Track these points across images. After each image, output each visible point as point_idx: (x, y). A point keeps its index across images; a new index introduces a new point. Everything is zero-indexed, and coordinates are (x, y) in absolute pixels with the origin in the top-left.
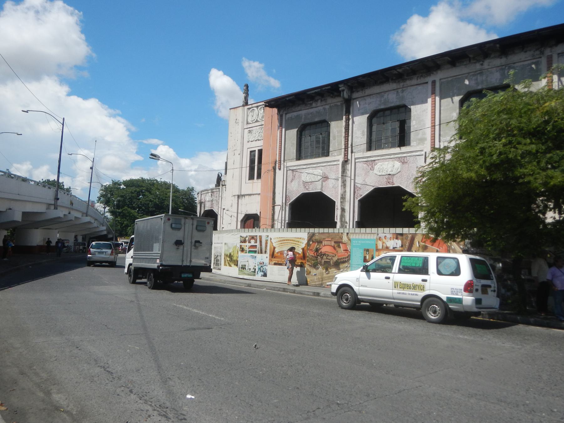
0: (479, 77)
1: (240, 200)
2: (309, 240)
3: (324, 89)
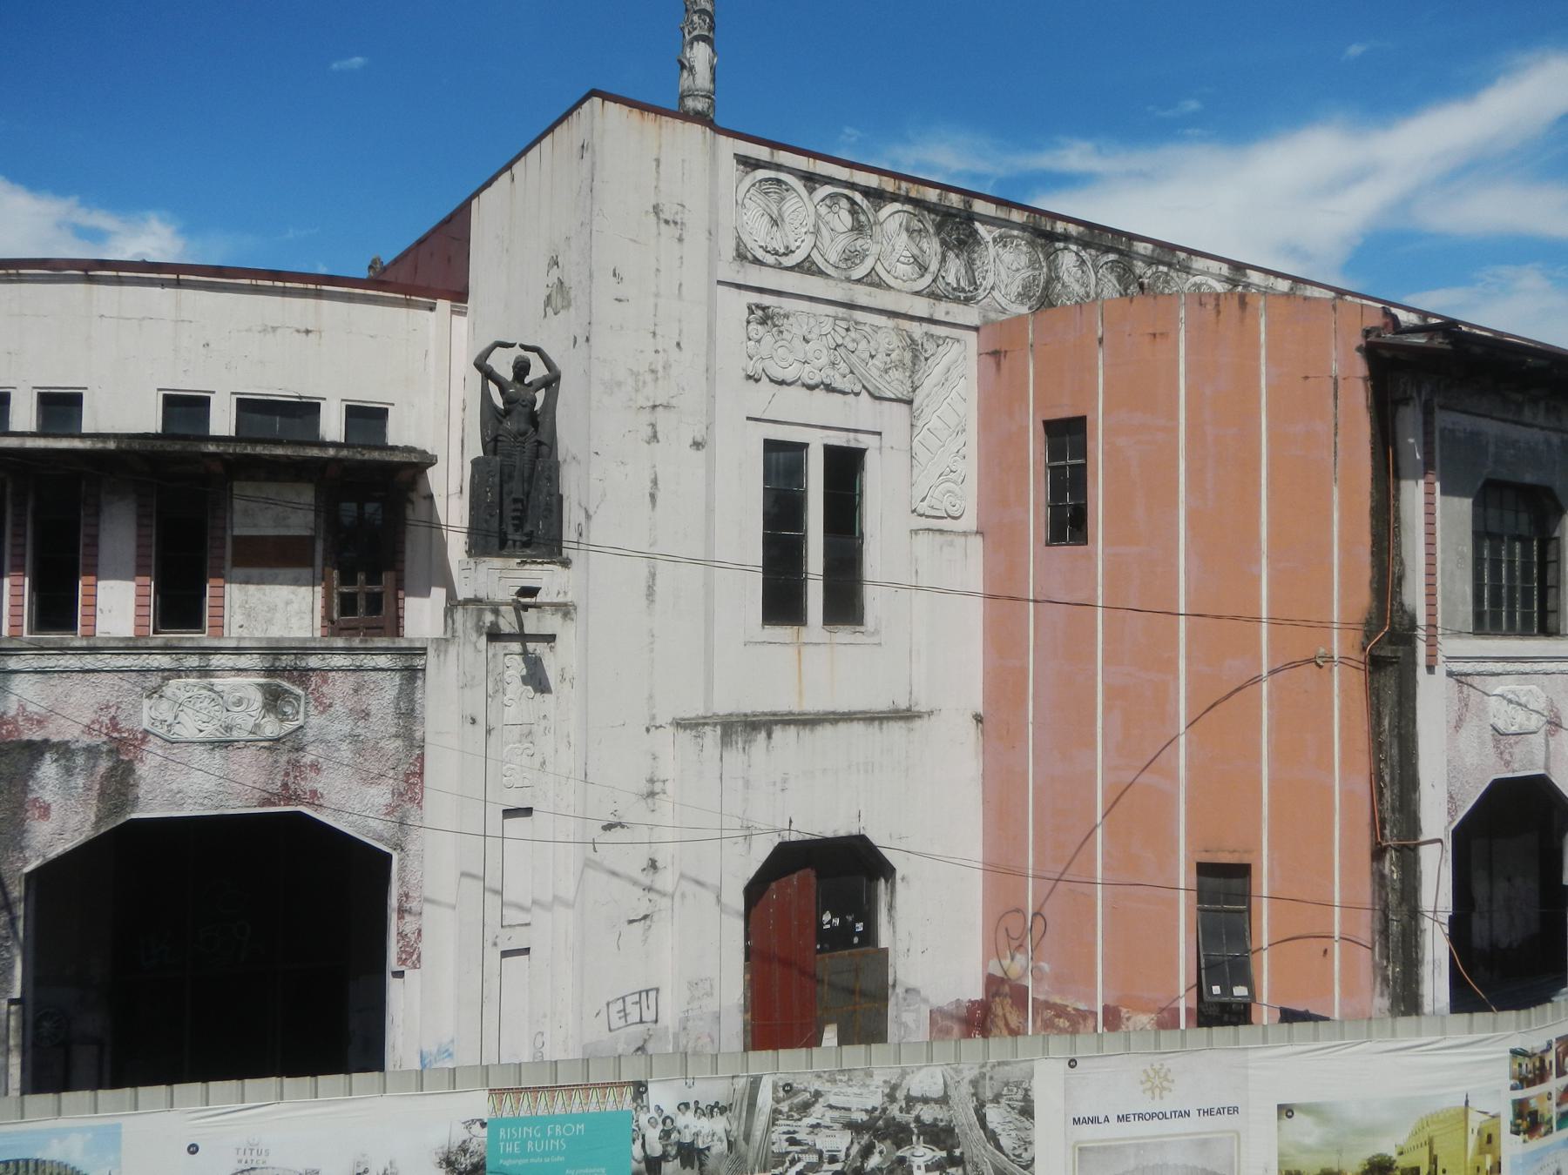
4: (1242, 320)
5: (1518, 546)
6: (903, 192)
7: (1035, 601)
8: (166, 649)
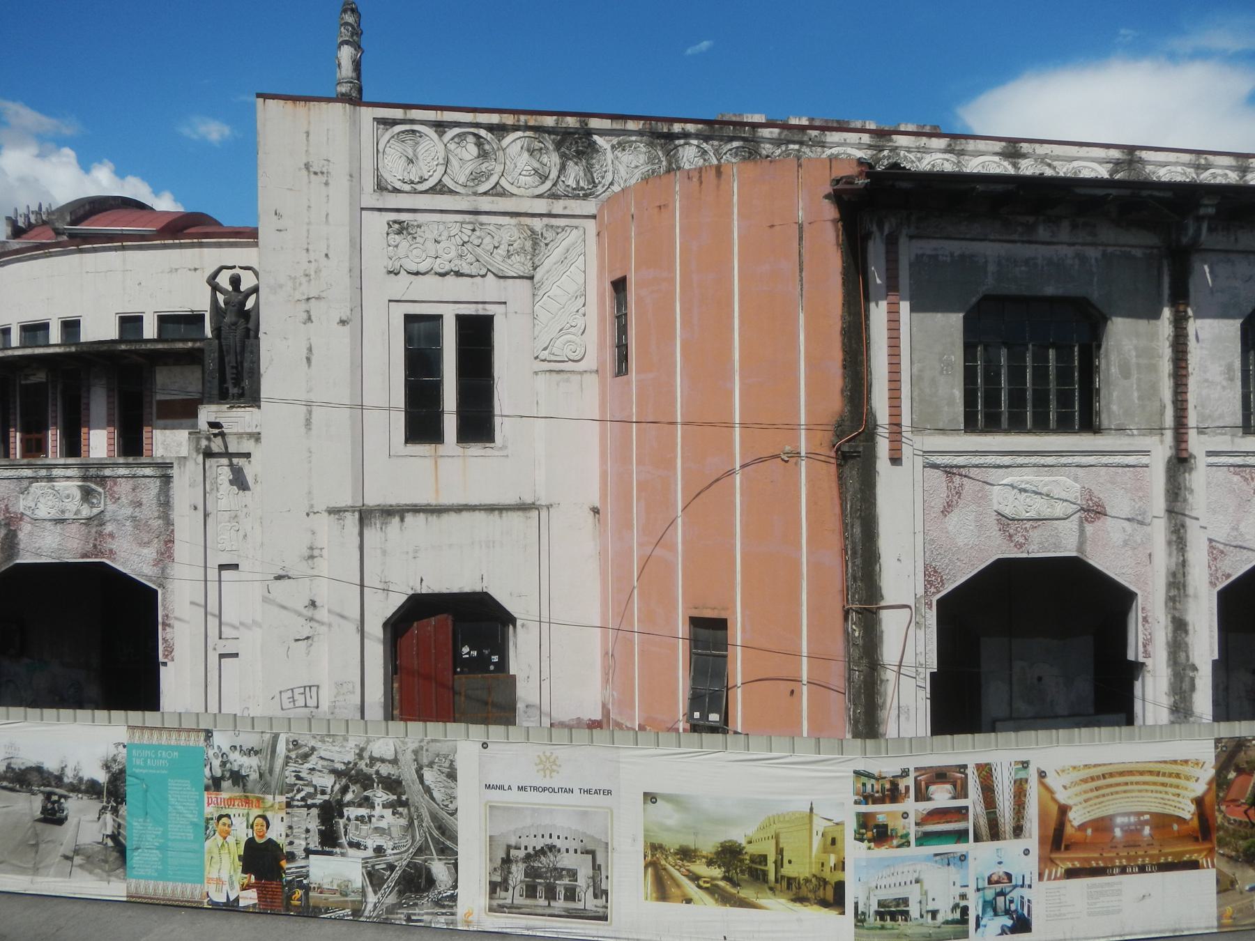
1: (365, 532)
2: (1222, 769)
3: (1145, 193)
4: (718, 186)
5: (1052, 353)
6: (521, 124)
7: (675, 423)
8: (29, 466)
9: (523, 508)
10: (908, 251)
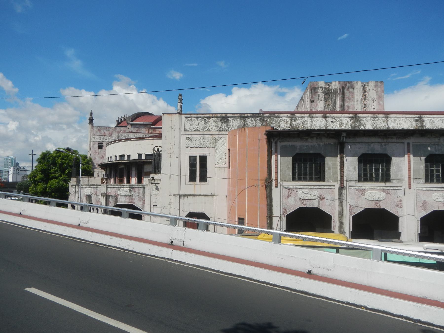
0: (437, 147)
1: (180, 200)
5: (313, 165)
8: (120, 185)
9: (212, 195)
10: (279, 145)
